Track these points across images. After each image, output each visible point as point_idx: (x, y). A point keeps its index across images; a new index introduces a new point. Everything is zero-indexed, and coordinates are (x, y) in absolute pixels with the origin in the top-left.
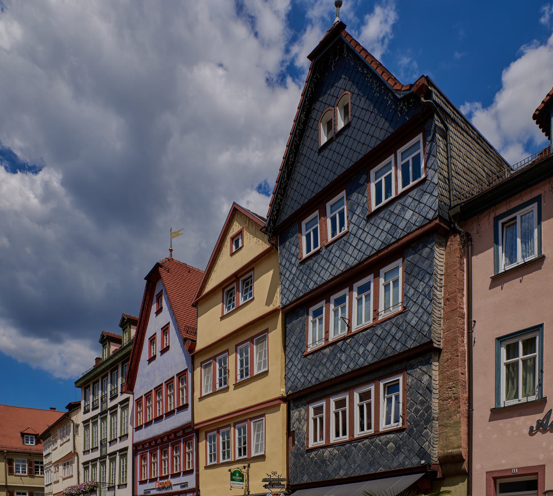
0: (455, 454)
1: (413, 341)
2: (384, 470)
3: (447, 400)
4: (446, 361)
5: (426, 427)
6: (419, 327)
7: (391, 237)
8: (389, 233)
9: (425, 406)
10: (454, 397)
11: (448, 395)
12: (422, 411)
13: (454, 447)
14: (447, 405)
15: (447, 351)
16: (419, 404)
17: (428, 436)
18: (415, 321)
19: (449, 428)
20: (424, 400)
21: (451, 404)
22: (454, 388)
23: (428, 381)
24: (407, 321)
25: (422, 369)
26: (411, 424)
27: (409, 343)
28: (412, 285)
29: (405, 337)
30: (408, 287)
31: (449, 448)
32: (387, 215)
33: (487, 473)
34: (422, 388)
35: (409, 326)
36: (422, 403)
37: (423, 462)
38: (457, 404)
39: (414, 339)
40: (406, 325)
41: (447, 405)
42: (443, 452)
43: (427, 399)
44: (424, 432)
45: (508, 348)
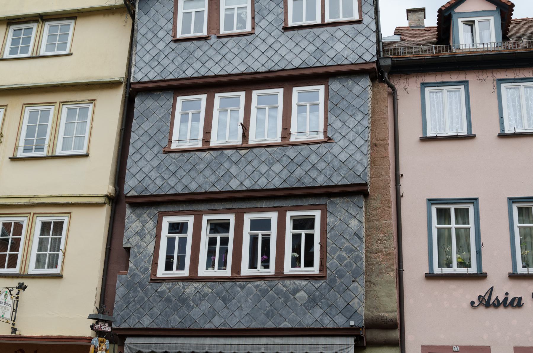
0: (388, 319)
1: (341, 177)
2: (290, 326)
3: (376, 253)
4: (375, 209)
5: (353, 279)
6: (351, 164)
7: (316, 60)
8: (313, 55)
9: (353, 255)
10: (386, 252)
11: (377, 247)
12: (348, 260)
13: (387, 310)
14: (376, 258)
15: (376, 198)
16: (344, 250)
17: (357, 292)
18: (345, 157)
19: (380, 287)
20: (351, 248)
21: (382, 258)
22: (385, 242)
23: (357, 227)
24: (334, 154)
25: (348, 211)
26: (333, 272)
27: (336, 179)
28: (340, 118)
29: (329, 170)
30: (333, 118)
31: (379, 310)
32: (311, 37)
33: (422, 346)
34: (349, 233)
35: (336, 159)
36: (350, 251)
37: (352, 323)
38: (389, 260)
39: (343, 175)
40: (331, 157)
41: (376, 258)
42: (371, 314)
43: (356, 246)
44: (352, 286)
45: (439, 211)
